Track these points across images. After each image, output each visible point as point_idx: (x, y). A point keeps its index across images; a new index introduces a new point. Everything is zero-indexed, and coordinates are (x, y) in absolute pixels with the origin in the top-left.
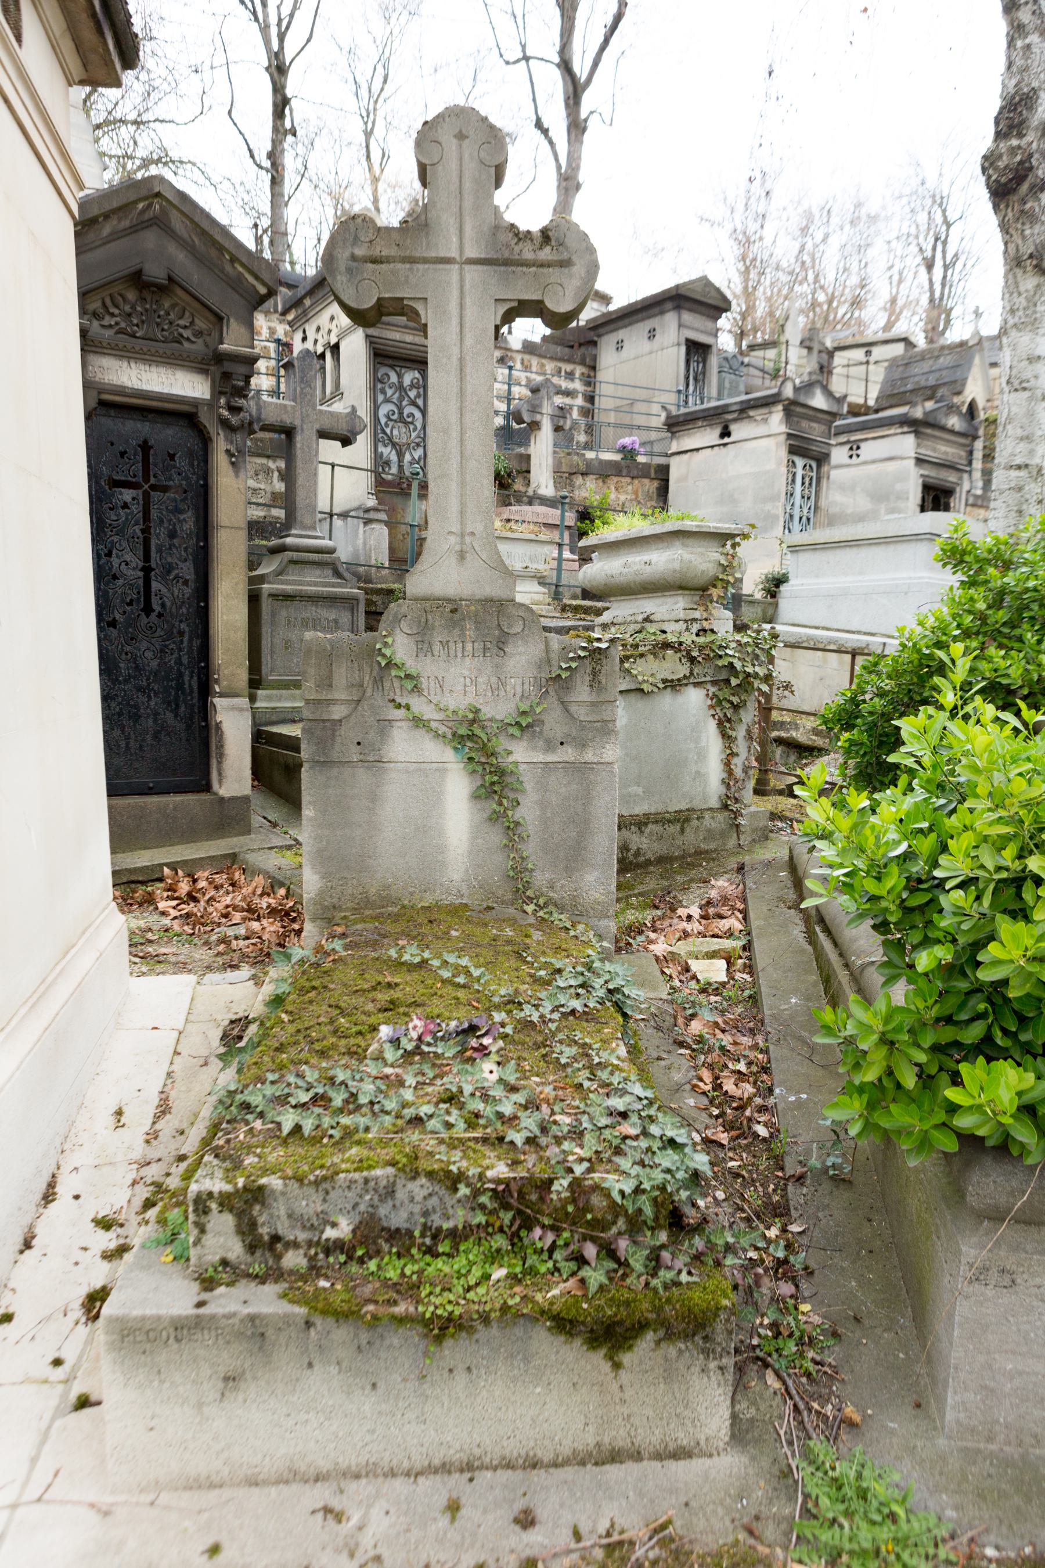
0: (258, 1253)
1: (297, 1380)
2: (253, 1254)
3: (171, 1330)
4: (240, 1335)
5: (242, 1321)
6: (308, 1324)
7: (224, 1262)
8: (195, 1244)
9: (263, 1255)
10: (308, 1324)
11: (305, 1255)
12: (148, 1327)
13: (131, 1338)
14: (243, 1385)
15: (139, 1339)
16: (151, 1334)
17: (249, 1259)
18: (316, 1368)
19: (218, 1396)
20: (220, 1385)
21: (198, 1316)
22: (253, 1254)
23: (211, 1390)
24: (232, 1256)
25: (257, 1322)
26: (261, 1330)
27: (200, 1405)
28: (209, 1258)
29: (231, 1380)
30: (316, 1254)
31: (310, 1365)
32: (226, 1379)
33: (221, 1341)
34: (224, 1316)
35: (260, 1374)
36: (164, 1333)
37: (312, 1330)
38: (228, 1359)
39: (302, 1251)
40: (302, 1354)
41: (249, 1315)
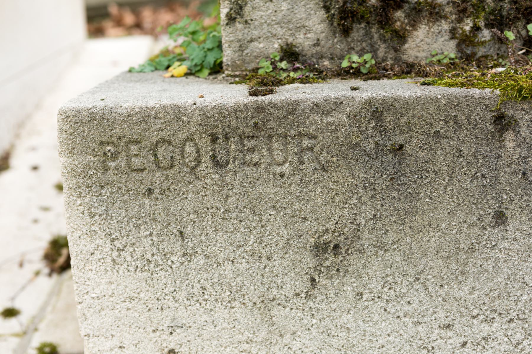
0: (358, 31)
1: (472, 250)
2: (346, 32)
3: (204, 142)
4: (350, 150)
5: (353, 117)
6: (502, 122)
7: (290, 54)
8: (231, 19)
9: (368, 34)
10: (502, 122)
11: (453, 32)
12: (155, 136)
13: (122, 161)
14: (355, 261)
15: (136, 162)
16: (161, 151)
17: (339, 45)
18: (512, 224)
19: (303, 285)
20: (309, 260)
21: (260, 109)
22: (346, 32)
23: (289, 270)
24: (303, 41)
25: (388, 118)
26: (399, 139)
27: (266, 303)
28: (259, 46)
29: (330, 251)
30: (476, 29)
31: (500, 218)
32: (320, 249)
33: (309, 166)
34: (316, 107)
35: (392, 236)
36: (189, 148)
37: (509, 135)
38: (324, 206)
39: (445, 26)
40: (484, 189)
41: (370, 102)
